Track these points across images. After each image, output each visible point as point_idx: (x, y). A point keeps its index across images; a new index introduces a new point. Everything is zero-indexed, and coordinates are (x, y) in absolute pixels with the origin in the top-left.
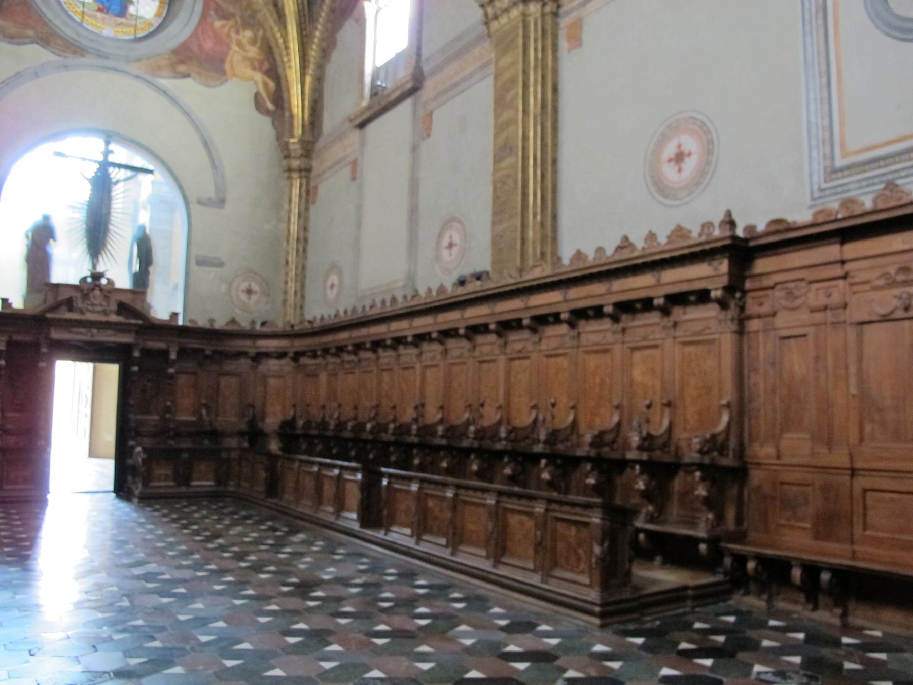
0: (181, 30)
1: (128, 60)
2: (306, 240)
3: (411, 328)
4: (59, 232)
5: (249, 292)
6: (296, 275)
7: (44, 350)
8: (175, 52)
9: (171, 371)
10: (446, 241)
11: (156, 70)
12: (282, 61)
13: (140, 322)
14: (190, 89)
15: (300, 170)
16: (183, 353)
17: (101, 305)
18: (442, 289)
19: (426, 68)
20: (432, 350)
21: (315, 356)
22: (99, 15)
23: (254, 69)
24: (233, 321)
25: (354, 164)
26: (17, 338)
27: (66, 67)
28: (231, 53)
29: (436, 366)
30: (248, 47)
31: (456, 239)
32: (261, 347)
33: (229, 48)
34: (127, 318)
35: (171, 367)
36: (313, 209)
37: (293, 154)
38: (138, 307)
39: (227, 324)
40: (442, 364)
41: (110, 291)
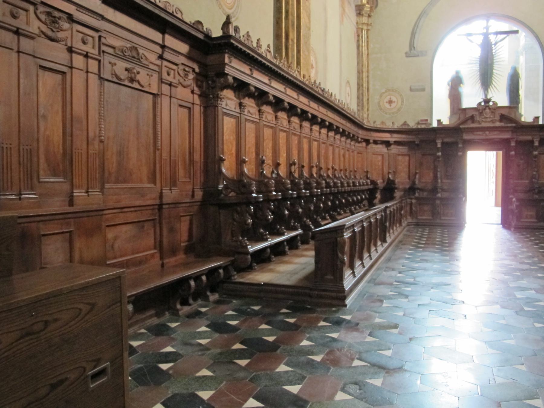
4: (465, 80)
7: (460, 145)
9: (536, 153)
13: (514, 125)
17: (490, 118)
26: (446, 140)
35: (536, 151)
38: (512, 116)
41: (496, 108)
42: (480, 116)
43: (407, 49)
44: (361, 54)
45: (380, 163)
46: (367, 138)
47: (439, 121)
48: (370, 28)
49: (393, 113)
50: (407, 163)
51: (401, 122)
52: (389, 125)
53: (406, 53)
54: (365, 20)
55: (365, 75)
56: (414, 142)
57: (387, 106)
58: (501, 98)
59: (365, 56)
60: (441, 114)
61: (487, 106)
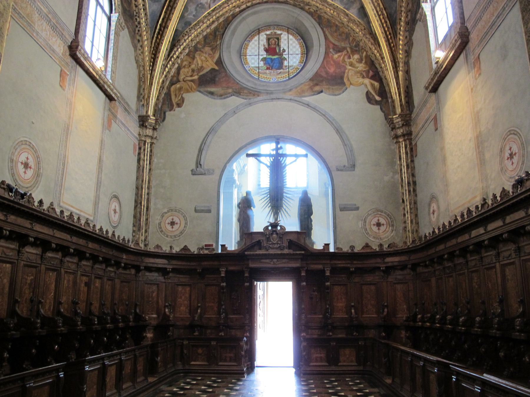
0: (314, 65)
1: (285, 92)
2: (415, 183)
3: (487, 232)
5: (379, 225)
6: (411, 209)
7: (247, 275)
8: (311, 80)
9: (328, 284)
10: (507, 155)
11: (301, 94)
12: (381, 68)
13: (303, 252)
14: (324, 100)
15: (403, 135)
16: (334, 270)
17: (278, 244)
18: (504, 192)
19: (469, 25)
20: (508, 250)
21: (426, 266)
22: (268, 71)
23: (363, 77)
24: (367, 246)
25: (435, 119)
26: (231, 268)
27: (250, 104)
28: (347, 71)
29: (513, 263)
30: (357, 65)
31: (515, 149)
32: (388, 263)
33: (346, 69)
34: (294, 251)
35: (328, 282)
36: (416, 160)
37: (397, 126)
38: (302, 242)
39: (363, 248)
40: (517, 261)
41: (285, 233)
42: (268, 241)
43: (193, 166)
44: (141, 168)
45: (155, 294)
46: (136, 263)
47: (223, 246)
48: (155, 141)
49: (175, 236)
50: (187, 295)
51: (182, 247)
52: (166, 249)
53: (192, 171)
54: (149, 132)
55: (145, 191)
56: (196, 270)
57: (169, 227)
58: (291, 223)
59: (146, 171)
60: (230, 239)
61: (274, 231)
